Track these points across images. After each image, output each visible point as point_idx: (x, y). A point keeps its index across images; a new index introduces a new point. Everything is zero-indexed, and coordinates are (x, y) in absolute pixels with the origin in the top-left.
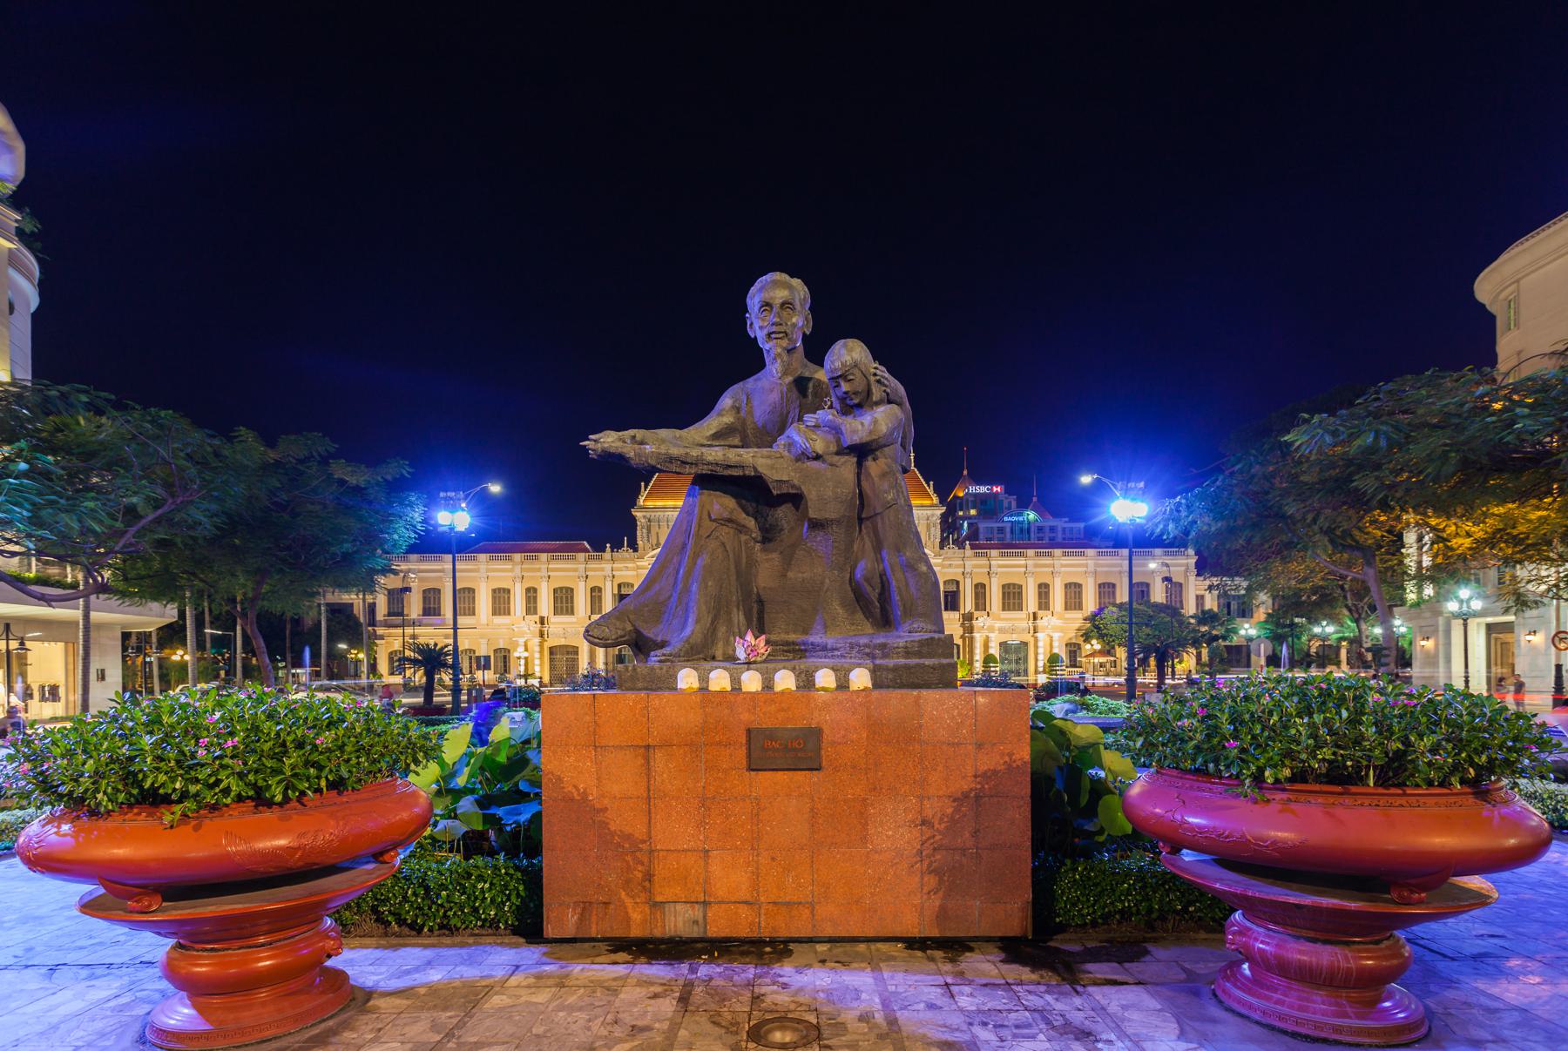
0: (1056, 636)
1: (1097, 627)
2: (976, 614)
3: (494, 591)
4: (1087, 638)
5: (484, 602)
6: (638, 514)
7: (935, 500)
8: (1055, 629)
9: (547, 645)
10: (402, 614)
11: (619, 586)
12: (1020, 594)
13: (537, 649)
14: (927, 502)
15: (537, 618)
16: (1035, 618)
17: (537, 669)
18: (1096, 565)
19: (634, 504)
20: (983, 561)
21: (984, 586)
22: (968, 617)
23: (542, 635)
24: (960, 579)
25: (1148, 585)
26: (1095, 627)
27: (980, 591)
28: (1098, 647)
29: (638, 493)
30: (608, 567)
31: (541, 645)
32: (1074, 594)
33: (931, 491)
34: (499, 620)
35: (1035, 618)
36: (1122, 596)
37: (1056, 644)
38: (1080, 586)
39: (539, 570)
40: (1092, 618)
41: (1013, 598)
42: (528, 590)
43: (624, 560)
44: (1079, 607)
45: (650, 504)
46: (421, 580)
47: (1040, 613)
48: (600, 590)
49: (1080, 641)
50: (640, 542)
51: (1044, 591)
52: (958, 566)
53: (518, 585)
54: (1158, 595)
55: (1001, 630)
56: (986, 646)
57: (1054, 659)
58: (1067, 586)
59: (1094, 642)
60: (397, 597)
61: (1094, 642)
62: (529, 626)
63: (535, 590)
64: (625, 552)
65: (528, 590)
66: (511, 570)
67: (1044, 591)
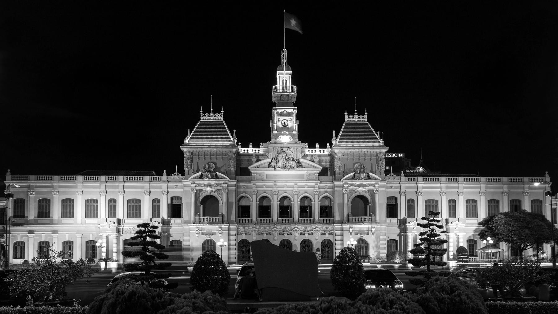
0: (461, 235)
1: (491, 229)
2: (409, 220)
3: (87, 201)
4: (483, 236)
5: (80, 209)
6: (185, 150)
7: (382, 143)
8: (461, 230)
9: (122, 238)
10: (24, 217)
11: (172, 199)
13: (115, 241)
14: (377, 144)
15: (115, 220)
17: (115, 255)
18: (486, 188)
19: (182, 143)
20: (413, 184)
21: (413, 201)
22: (403, 222)
23: (118, 231)
24: (398, 196)
25: (520, 201)
26: (488, 228)
27: (411, 204)
28: (491, 242)
29: (186, 136)
30: (164, 185)
31: (118, 239)
32: (472, 206)
33: (378, 136)
34: (90, 221)
36: (504, 208)
37: (461, 240)
38: (476, 201)
39: (118, 187)
40: (485, 223)
42: (110, 201)
43: (175, 181)
44: (475, 215)
46: (37, 193)
47: (451, 219)
48: (159, 201)
49: (477, 239)
50: (186, 169)
51: (452, 204)
52: (396, 188)
53: (103, 197)
54: (527, 207)
57: (460, 250)
58: (468, 201)
59: (489, 239)
60: (20, 206)
61: (489, 239)
62: (111, 224)
63: (115, 201)
64: (176, 176)
65: (110, 201)
66: (99, 187)
67: (452, 204)
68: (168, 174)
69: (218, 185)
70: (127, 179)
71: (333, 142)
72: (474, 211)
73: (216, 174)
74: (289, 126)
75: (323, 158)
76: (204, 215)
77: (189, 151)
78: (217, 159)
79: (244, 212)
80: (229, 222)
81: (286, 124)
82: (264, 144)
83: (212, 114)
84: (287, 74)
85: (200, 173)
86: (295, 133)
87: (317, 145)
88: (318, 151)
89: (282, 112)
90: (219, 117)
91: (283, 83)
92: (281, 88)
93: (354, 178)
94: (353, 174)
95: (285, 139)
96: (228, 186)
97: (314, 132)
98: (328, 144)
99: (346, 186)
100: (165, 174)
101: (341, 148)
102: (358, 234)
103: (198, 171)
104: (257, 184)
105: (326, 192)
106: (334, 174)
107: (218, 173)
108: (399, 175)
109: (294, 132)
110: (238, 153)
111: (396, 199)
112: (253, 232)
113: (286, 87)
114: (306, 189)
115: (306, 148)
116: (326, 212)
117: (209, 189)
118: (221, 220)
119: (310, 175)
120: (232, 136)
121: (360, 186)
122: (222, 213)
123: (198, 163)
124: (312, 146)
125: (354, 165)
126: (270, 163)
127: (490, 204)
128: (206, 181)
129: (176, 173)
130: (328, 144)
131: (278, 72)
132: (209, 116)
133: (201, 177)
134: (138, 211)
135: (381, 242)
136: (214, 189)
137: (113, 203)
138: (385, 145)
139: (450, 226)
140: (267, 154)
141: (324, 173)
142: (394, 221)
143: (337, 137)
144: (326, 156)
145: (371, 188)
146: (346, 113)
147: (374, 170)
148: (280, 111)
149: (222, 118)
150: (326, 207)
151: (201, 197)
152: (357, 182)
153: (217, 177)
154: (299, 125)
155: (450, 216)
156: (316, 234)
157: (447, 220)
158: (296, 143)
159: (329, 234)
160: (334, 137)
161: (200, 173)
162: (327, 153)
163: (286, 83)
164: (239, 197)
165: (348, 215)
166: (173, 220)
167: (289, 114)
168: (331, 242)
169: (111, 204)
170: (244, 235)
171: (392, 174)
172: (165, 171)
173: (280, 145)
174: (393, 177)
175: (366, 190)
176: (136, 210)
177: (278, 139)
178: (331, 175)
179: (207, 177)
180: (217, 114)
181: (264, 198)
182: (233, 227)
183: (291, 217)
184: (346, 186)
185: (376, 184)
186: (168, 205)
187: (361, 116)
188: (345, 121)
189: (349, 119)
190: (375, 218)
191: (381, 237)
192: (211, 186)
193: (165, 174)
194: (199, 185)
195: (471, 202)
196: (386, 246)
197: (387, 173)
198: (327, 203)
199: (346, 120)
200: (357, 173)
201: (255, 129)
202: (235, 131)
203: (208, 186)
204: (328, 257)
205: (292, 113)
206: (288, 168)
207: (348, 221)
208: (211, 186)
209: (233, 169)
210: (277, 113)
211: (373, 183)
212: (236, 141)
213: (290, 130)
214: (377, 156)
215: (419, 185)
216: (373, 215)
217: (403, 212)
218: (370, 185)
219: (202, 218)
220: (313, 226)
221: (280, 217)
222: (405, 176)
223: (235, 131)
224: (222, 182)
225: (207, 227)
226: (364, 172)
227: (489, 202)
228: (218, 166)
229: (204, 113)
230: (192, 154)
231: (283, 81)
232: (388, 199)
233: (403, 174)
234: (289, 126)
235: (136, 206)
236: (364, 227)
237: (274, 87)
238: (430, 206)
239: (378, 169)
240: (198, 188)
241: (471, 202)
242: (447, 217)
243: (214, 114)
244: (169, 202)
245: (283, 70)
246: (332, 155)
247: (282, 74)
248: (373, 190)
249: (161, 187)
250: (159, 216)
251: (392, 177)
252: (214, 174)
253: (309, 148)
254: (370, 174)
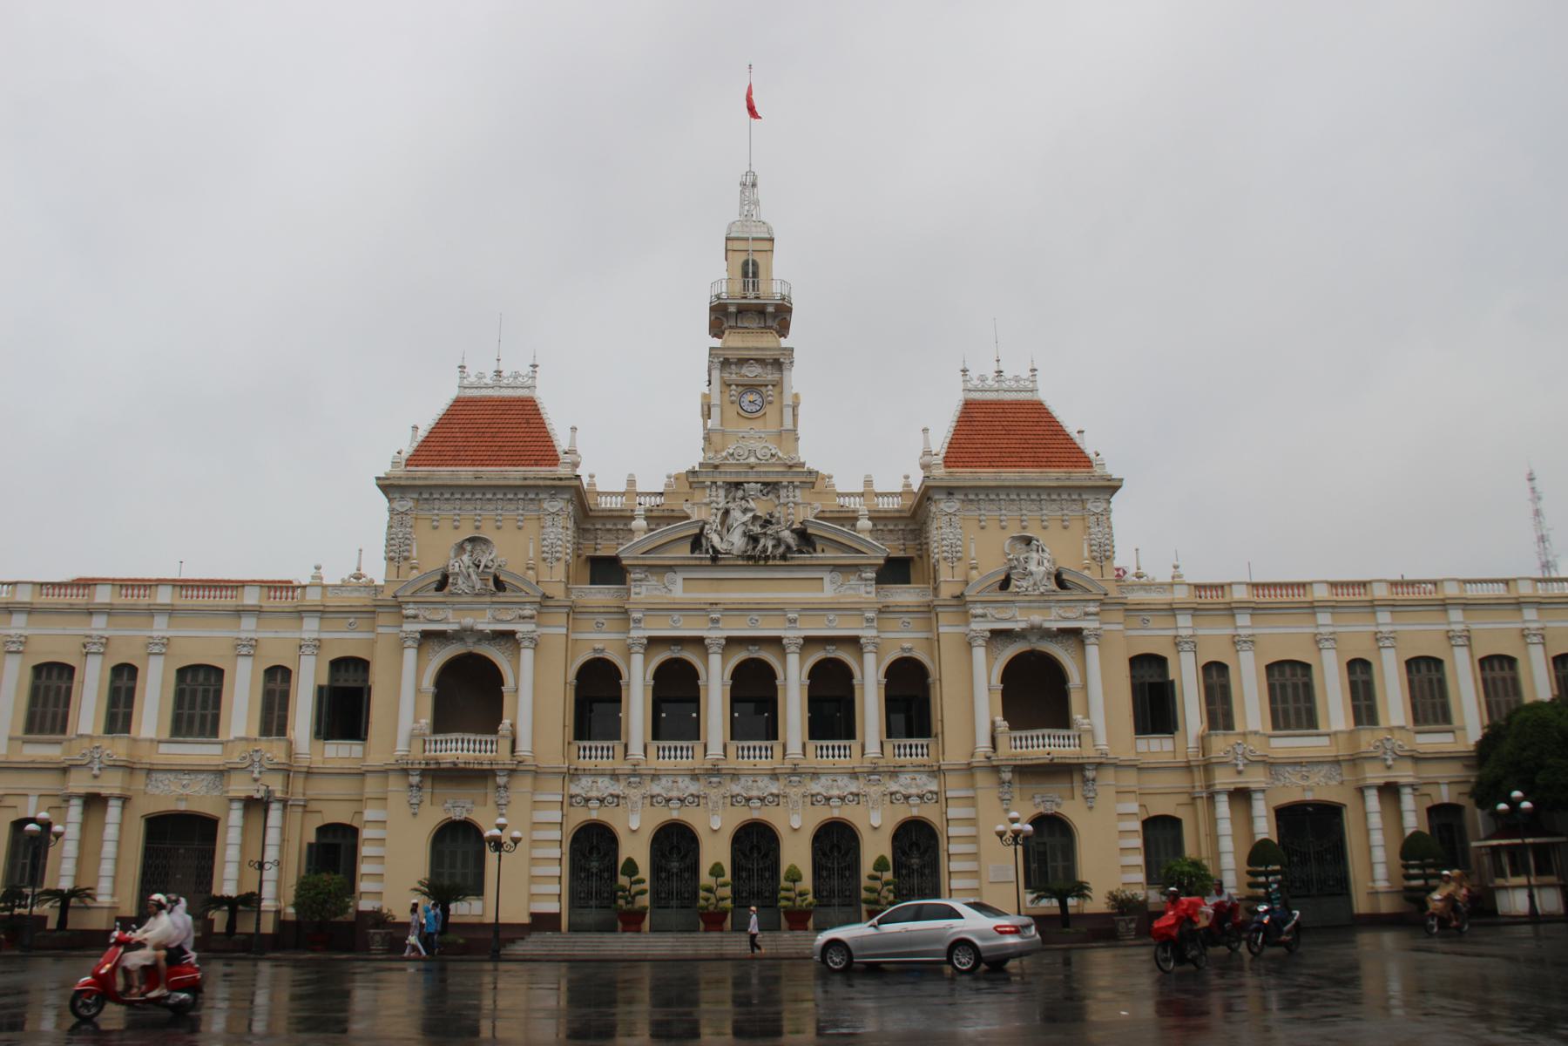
27: (1216, 676)
72: (1438, 700)
127: (1489, 674)
134: (209, 712)
137: (124, 682)
169: (119, 683)
176: (204, 707)
183: (775, 737)
195: (1423, 668)
196: (1138, 842)
227: (1482, 668)
232: (1138, 662)
235: (206, 691)
238: (1283, 687)
241: (1423, 668)
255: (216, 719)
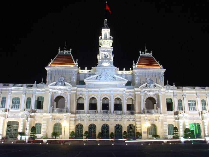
6: (47, 69)
7: (161, 67)
11: (38, 98)
12: (195, 104)
14: (158, 68)
16: (202, 113)
19: (47, 65)
24: (172, 97)
31: (4, 121)
33: (159, 64)
35: (202, 113)
41: (192, 105)
45: (53, 65)
47: (204, 111)
50: (47, 80)
55: (190, 119)
56: (184, 125)
64: (42, 84)
68: (38, 83)
69: (65, 89)
70: (14, 86)
71: (134, 67)
73: (65, 84)
74: (108, 57)
75: (128, 76)
76: (57, 107)
77: (50, 70)
78: (66, 75)
79: (80, 107)
80: (72, 113)
81: (107, 56)
82: (94, 68)
83: (65, 51)
84: (107, 31)
85: (55, 83)
86: (112, 61)
87: (124, 69)
88: (124, 72)
89: (104, 50)
90: (69, 52)
91: (105, 35)
92: (104, 37)
93: (146, 86)
94: (146, 84)
95: (106, 64)
96: (71, 91)
97: (123, 60)
98: (130, 69)
99: (142, 91)
100: (35, 83)
101: (138, 70)
102: (150, 120)
103: (54, 81)
104: (89, 89)
105: (130, 95)
106: (134, 84)
107: (66, 83)
108: (172, 85)
109: (111, 61)
110: (78, 73)
111: (171, 99)
112: (86, 119)
113: (107, 37)
114: (118, 93)
115: (118, 70)
116: (130, 107)
117: (60, 92)
118: (66, 111)
119: (121, 84)
120: (76, 62)
121: (150, 91)
122: (67, 107)
123: (54, 77)
124: (121, 69)
125: (146, 79)
126: (97, 78)
128: (58, 87)
129: (42, 83)
130: (130, 69)
131: (102, 30)
132: (63, 52)
133: (55, 85)
135: (165, 126)
136: (63, 92)
138: (163, 68)
139: (204, 115)
140: (95, 73)
141: (128, 84)
142: (170, 112)
143: (135, 64)
144: (130, 75)
145: (157, 92)
146: (140, 52)
147: (158, 82)
148: (103, 49)
149: (70, 53)
150: (130, 105)
151: (55, 97)
152: (148, 89)
153: (65, 85)
154: (114, 57)
155: (203, 110)
156: (125, 120)
157: (201, 112)
158: (112, 66)
159: (132, 120)
160: (134, 64)
161: (55, 83)
162: (130, 73)
163: (107, 35)
164: (78, 97)
165: (144, 109)
166: (38, 110)
167: (108, 51)
168: (134, 126)
170: (80, 121)
171: (168, 85)
172: (36, 81)
173: (103, 68)
174: (168, 86)
175: (154, 94)
177: (102, 65)
178: (133, 85)
179: (59, 85)
180: (68, 51)
181: (93, 98)
182: (73, 115)
184: (142, 91)
185: (160, 90)
186: (36, 101)
187: (149, 53)
188: (140, 56)
189: (142, 55)
190: (160, 111)
191: (164, 123)
192: (60, 90)
193: (35, 83)
194: (54, 89)
197: (165, 84)
198: (130, 103)
199: (140, 55)
200: (148, 84)
201: (88, 60)
202: (77, 60)
203: (60, 90)
204: (132, 135)
205: (110, 50)
206: (107, 80)
207: (144, 113)
208: (60, 90)
209: (75, 81)
210: (102, 50)
211: (158, 89)
212: (77, 66)
213: (109, 59)
214: (159, 74)
215: (184, 91)
216: (159, 109)
217: (176, 108)
218: (157, 91)
219: (55, 109)
220: (123, 116)
221: (102, 110)
222: (176, 86)
223: (77, 60)
224: (67, 88)
225: (57, 115)
226: (152, 83)
228: (66, 79)
229: (61, 50)
230: (52, 72)
231: (105, 34)
233: (174, 85)
234: (108, 57)
236: (154, 116)
237: (100, 37)
239: (160, 82)
240: (54, 91)
242: (202, 110)
243: (66, 51)
244: (37, 100)
245: (105, 29)
246: (132, 74)
247: (105, 31)
248: (158, 94)
249: (32, 91)
250: (30, 108)
251: (168, 87)
252: (64, 83)
253: (120, 70)
254: (156, 84)
255: (19, 106)
